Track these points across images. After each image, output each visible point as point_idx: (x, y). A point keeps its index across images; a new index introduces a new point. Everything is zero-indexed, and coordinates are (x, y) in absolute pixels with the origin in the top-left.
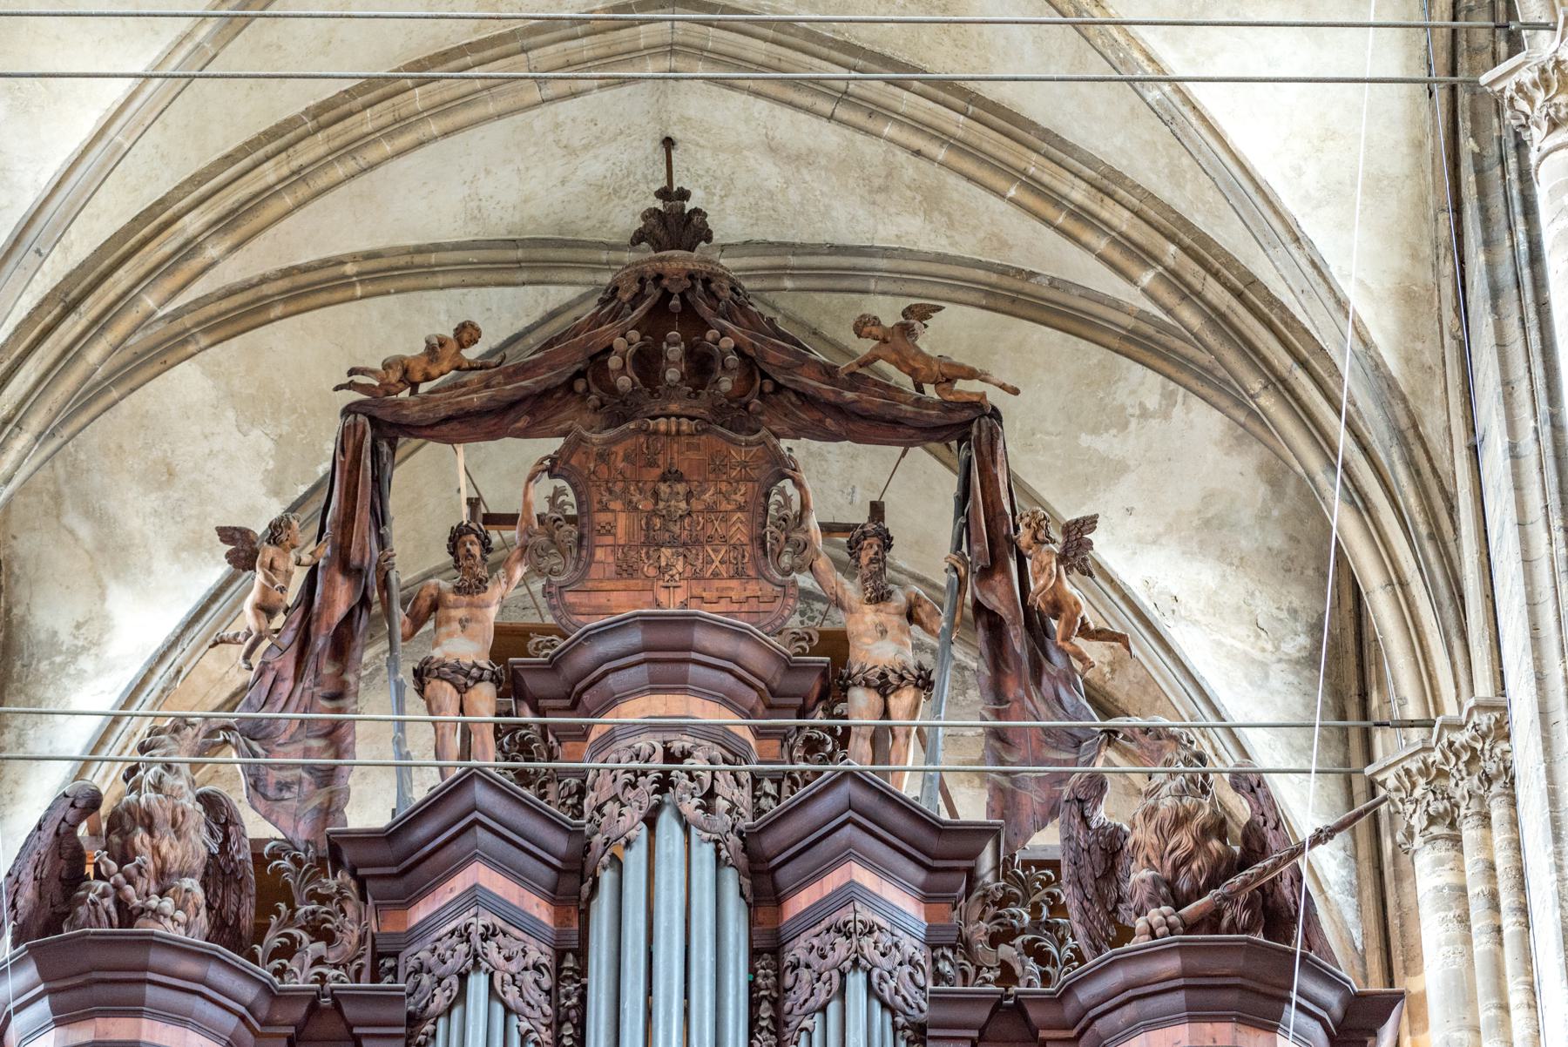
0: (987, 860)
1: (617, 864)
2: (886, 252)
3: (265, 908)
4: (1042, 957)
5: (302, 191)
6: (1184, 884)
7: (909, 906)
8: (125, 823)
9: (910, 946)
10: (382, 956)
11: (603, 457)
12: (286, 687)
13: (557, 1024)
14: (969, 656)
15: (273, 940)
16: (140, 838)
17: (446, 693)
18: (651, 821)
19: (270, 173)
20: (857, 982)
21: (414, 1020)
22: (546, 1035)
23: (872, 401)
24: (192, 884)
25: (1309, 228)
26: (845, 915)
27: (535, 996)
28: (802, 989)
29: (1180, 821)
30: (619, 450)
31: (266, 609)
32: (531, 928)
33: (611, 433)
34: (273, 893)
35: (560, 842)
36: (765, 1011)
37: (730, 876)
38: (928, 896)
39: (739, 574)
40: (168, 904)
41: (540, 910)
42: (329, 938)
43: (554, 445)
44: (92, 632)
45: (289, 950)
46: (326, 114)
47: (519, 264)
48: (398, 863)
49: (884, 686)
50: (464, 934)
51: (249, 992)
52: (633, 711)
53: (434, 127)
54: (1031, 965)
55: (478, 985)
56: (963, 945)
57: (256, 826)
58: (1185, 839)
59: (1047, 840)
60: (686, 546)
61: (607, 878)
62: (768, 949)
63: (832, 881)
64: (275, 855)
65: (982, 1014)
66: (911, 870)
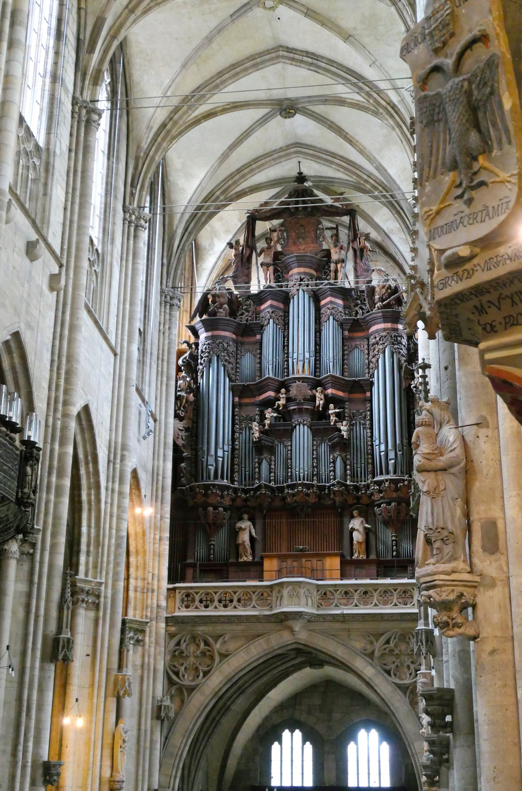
0: (353, 292)
1: (293, 298)
2: (338, 179)
3: (238, 307)
4: (362, 308)
5: (236, 185)
6: (384, 298)
7: (340, 302)
8: (214, 296)
9: (341, 309)
10: (257, 313)
11: (290, 223)
12: (240, 268)
13: (284, 326)
14: (351, 253)
15: (240, 313)
16: (217, 299)
17: (265, 267)
18: (298, 290)
19: (230, 182)
20: (331, 317)
21: (262, 326)
22: (283, 327)
23: (334, 210)
24: (226, 306)
25: (401, 187)
26: (329, 306)
27: (282, 321)
28: (324, 318)
29: (383, 287)
30: (293, 221)
31: (235, 256)
32: (280, 309)
33: (291, 218)
34: (240, 304)
35: (284, 294)
36: (318, 321)
37: (311, 299)
38: (343, 300)
39: (313, 243)
40: (222, 310)
41: (281, 306)
42: (248, 312)
43: (282, 220)
44: (212, 245)
45: (242, 314)
46: (239, 171)
47: (276, 184)
48: (259, 298)
49: (336, 263)
50: (269, 312)
51: (235, 324)
52: (295, 270)
53: (257, 171)
54: (361, 311)
55: (271, 321)
56: (349, 308)
57: (236, 292)
58: (384, 290)
59: (363, 287)
60: (304, 239)
61: (292, 300)
62: (318, 309)
63: (328, 299)
64: (240, 298)
65: (352, 322)
66: (340, 296)
